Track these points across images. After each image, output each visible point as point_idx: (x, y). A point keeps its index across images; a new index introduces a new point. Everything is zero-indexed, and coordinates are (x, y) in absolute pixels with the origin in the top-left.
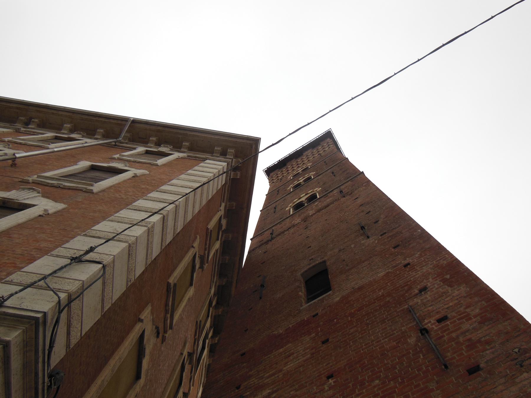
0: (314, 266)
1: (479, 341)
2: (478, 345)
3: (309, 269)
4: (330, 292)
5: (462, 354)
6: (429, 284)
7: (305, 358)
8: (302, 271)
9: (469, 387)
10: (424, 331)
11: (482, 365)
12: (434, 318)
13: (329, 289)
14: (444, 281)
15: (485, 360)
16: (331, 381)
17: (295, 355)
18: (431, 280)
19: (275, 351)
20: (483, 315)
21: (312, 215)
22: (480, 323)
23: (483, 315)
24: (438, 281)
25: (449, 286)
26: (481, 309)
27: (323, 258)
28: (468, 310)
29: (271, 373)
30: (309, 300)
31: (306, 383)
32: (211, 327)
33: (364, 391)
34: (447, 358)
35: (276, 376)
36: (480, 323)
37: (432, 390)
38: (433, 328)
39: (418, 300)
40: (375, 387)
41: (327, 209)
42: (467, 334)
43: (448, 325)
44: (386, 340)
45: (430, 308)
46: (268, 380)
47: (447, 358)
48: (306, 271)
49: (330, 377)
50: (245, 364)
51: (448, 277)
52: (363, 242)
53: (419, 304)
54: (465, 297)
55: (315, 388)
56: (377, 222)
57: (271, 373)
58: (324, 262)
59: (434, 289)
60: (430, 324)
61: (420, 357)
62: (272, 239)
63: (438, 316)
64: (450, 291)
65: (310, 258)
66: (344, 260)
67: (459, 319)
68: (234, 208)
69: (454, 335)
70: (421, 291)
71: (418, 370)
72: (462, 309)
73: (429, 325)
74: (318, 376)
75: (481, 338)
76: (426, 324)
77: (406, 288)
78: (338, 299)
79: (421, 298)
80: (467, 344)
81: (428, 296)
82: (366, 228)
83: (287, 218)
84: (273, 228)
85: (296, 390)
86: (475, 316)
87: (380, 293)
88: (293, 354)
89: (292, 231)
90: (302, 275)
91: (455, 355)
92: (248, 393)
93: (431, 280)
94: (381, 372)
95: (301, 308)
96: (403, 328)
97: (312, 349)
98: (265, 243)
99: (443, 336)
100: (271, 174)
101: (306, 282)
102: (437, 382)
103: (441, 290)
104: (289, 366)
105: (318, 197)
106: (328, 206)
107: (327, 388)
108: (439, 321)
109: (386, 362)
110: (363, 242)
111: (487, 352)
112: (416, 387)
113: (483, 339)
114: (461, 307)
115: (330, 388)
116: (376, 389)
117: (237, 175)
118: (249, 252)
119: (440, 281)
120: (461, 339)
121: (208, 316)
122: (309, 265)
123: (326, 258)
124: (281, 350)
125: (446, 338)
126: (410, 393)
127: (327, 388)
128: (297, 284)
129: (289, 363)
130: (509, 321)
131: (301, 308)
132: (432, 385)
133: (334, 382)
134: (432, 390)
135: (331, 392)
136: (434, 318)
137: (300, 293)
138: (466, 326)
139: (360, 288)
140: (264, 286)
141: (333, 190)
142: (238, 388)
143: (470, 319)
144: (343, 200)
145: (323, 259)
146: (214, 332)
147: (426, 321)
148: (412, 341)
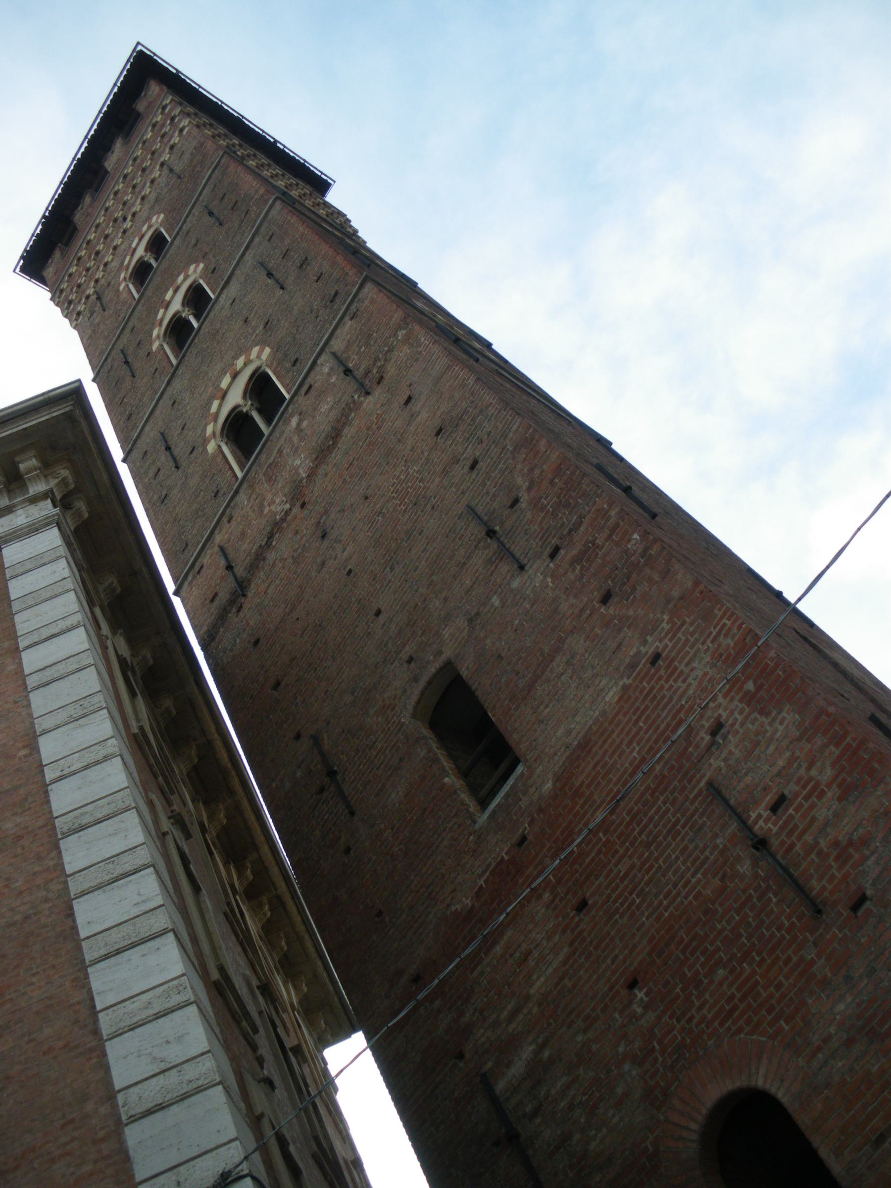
0: (429, 683)
1: (851, 843)
2: (851, 850)
3: (422, 693)
4: (520, 769)
5: (833, 877)
6: (724, 715)
7: (561, 958)
8: (410, 708)
9: (863, 940)
10: (761, 844)
11: (869, 893)
12: (764, 804)
13: (516, 762)
14: (748, 699)
15: (871, 881)
16: (640, 995)
17: (536, 954)
18: (720, 699)
19: (486, 954)
20: (840, 779)
21: (312, 475)
22: (840, 799)
23: (840, 779)
24: (736, 702)
25: (762, 712)
26: (833, 765)
27: (440, 653)
28: (813, 772)
29: (509, 1007)
30: (483, 804)
31: (593, 1010)
32: (226, 864)
33: (707, 996)
34: (814, 892)
35: (525, 1011)
36: (840, 799)
37: (812, 963)
38: (770, 830)
39: (716, 762)
40: (721, 984)
41: (343, 444)
42: (829, 830)
43: (791, 817)
44: (699, 876)
45: (748, 779)
46: (512, 1026)
47: (814, 892)
48: (418, 702)
49: (632, 985)
50: (437, 1003)
51: (750, 686)
52: (515, 584)
53: (723, 771)
54: (799, 739)
55: (617, 1015)
56: (516, 501)
57: (509, 1007)
58: (449, 665)
59: (737, 726)
60: (761, 820)
61: (770, 900)
62: (242, 587)
63: (770, 799)
64: (768, 728)
65: (404, 656)
66: (500, 656)
67: (807, 798)
68: (119, 590)
69: (808, 838)
70: (714, 733)
71: (779, 929)
72: (802, 771)
73: (761, 823)
74: (610, 989)
75: (852, 834)
76: (756, 822)
78: (549, 785)
79: (723, 756)
80: (835, 853)
81: (733, 746)
82: (497, 528)
83: (237, 492)
84: (218, 538)
85: (585, 1031)
86: (829, 785)
87: (635, 754)
88: (529, 953)
89: (284, 547)
90: (414, 716)
91: (824, 882)
92: (490, 1064)
93: (720, 699)
94: (718, 949)
95: (477, 826)
96: (718, 841)
97: (564, 931)
98: (232, 602)
99: (793, 845)
100: (49, 272)
101: (434, 725)
102: (815, 944)
103: (750, 726)
104: (538, 983)
105: (287, 396)
106: (335, 435)
107: (639, 1010)
108: (774, 808)
109: (719, 927)
110: (515, 584)
111: (869, 863)
112: (786, 963)
113: (855, 837)
114: (800, 766)
115: (646, 1007)
116: (725, 987)
117: (79, 513)
118: (204, 647)
119: (741, 701)
120: (823, 844)
121: (211, 854)
122: (416, 679)
123: (448, 653)
124: (498, 949)
125: (798, 847)
126: (781, 978)
127: (639, 1010)
128: (423, 753)
129: (535, 977)
130: (882, 786)
131: (477, 826)
132: (810, 954)
133: (647, 994)
134: (812, 963)
135: (651, 1016)
136: (764, 804)
137: (446, 780)
138: (822, 813)
139: (585, 746)
140: (335, 773)
141: (314, 363)
142: (461, 1056)
143: (823, 793)
144: (369, 403)
145: (444, 657)
146: (236, 867)
147: (754, 815)
148: (744, 868)
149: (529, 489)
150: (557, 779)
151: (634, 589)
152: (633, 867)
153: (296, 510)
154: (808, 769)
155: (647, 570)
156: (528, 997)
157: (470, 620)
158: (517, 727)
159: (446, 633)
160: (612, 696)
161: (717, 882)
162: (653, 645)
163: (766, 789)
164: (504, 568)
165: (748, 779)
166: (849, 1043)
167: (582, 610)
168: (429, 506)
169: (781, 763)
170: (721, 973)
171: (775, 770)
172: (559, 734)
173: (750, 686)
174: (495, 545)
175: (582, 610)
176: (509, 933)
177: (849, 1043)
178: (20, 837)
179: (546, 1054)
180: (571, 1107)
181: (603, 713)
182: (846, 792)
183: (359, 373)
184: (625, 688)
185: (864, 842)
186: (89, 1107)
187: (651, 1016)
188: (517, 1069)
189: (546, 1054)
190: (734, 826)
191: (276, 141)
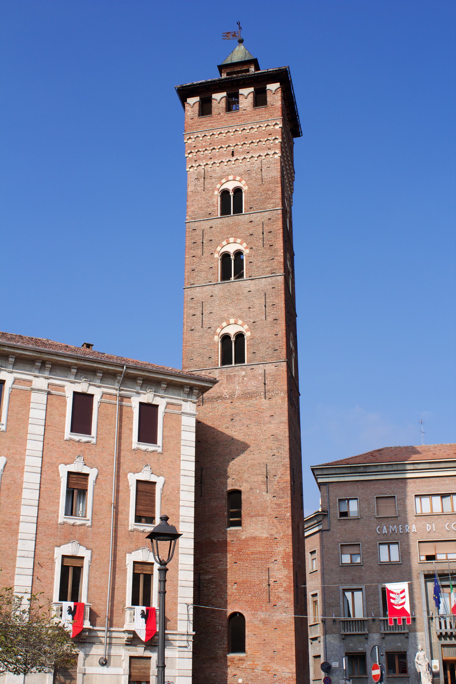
10: (269, 585)
14: (283, 562)
45: (274, 573)
46: (210, 570)
51: (285, 561)
60: (271, 582)
63: (275, 580)
66: (251, 503)
69: (276, 591)
77: (271, 554)
78: (243, 537)
88: (221, 561)
123: (242, 489)
124: (216, 554)
132: (264, 606)
139: (254, 538)
141: (259, 364)
143: (282, 587)
148: (264, 585)
149: (279, 478)
150: (246, 538)
151: (281, 523)
152: (248, 566)
153: (229, 401)
154: (284, 582)
155: (286, 522)
156: (216, 568)
157: (250, 489)
158: (245, 520)
159: (244, 484)
160: (265, 535)
161: (259, 582)
162: (276, 536)
163: (275, 578)
164: (264, 487)
165: (274, 573)
166: (260, 621)
167: (271, 515)
168: (259, 451)
169: (280, 577)
170: (250, 595)
171: (279, 577)
172: (252, 531)
173: (285, 561)
174: (266, 480)
175: (271, 515)
176: (220, 554)
177: (260, 621)
178: (173, 515)
179: (214, 580)
180: (213, 591)
181: (261, 537)
182: (285, 590)
183: (267, 388)
184: (268, 537)
185: (282, 599)
186: (174, 579)
187: (235, 591)
188: (207, 577)
189: (214, 580)
190: (267, 578)
191: (298, 115)
